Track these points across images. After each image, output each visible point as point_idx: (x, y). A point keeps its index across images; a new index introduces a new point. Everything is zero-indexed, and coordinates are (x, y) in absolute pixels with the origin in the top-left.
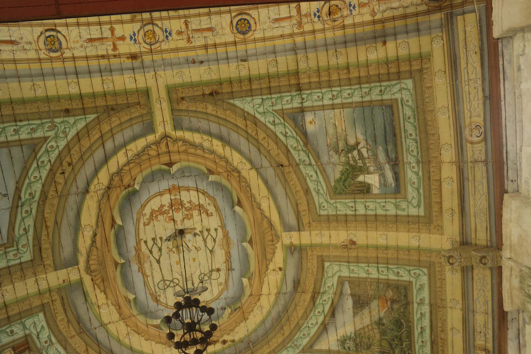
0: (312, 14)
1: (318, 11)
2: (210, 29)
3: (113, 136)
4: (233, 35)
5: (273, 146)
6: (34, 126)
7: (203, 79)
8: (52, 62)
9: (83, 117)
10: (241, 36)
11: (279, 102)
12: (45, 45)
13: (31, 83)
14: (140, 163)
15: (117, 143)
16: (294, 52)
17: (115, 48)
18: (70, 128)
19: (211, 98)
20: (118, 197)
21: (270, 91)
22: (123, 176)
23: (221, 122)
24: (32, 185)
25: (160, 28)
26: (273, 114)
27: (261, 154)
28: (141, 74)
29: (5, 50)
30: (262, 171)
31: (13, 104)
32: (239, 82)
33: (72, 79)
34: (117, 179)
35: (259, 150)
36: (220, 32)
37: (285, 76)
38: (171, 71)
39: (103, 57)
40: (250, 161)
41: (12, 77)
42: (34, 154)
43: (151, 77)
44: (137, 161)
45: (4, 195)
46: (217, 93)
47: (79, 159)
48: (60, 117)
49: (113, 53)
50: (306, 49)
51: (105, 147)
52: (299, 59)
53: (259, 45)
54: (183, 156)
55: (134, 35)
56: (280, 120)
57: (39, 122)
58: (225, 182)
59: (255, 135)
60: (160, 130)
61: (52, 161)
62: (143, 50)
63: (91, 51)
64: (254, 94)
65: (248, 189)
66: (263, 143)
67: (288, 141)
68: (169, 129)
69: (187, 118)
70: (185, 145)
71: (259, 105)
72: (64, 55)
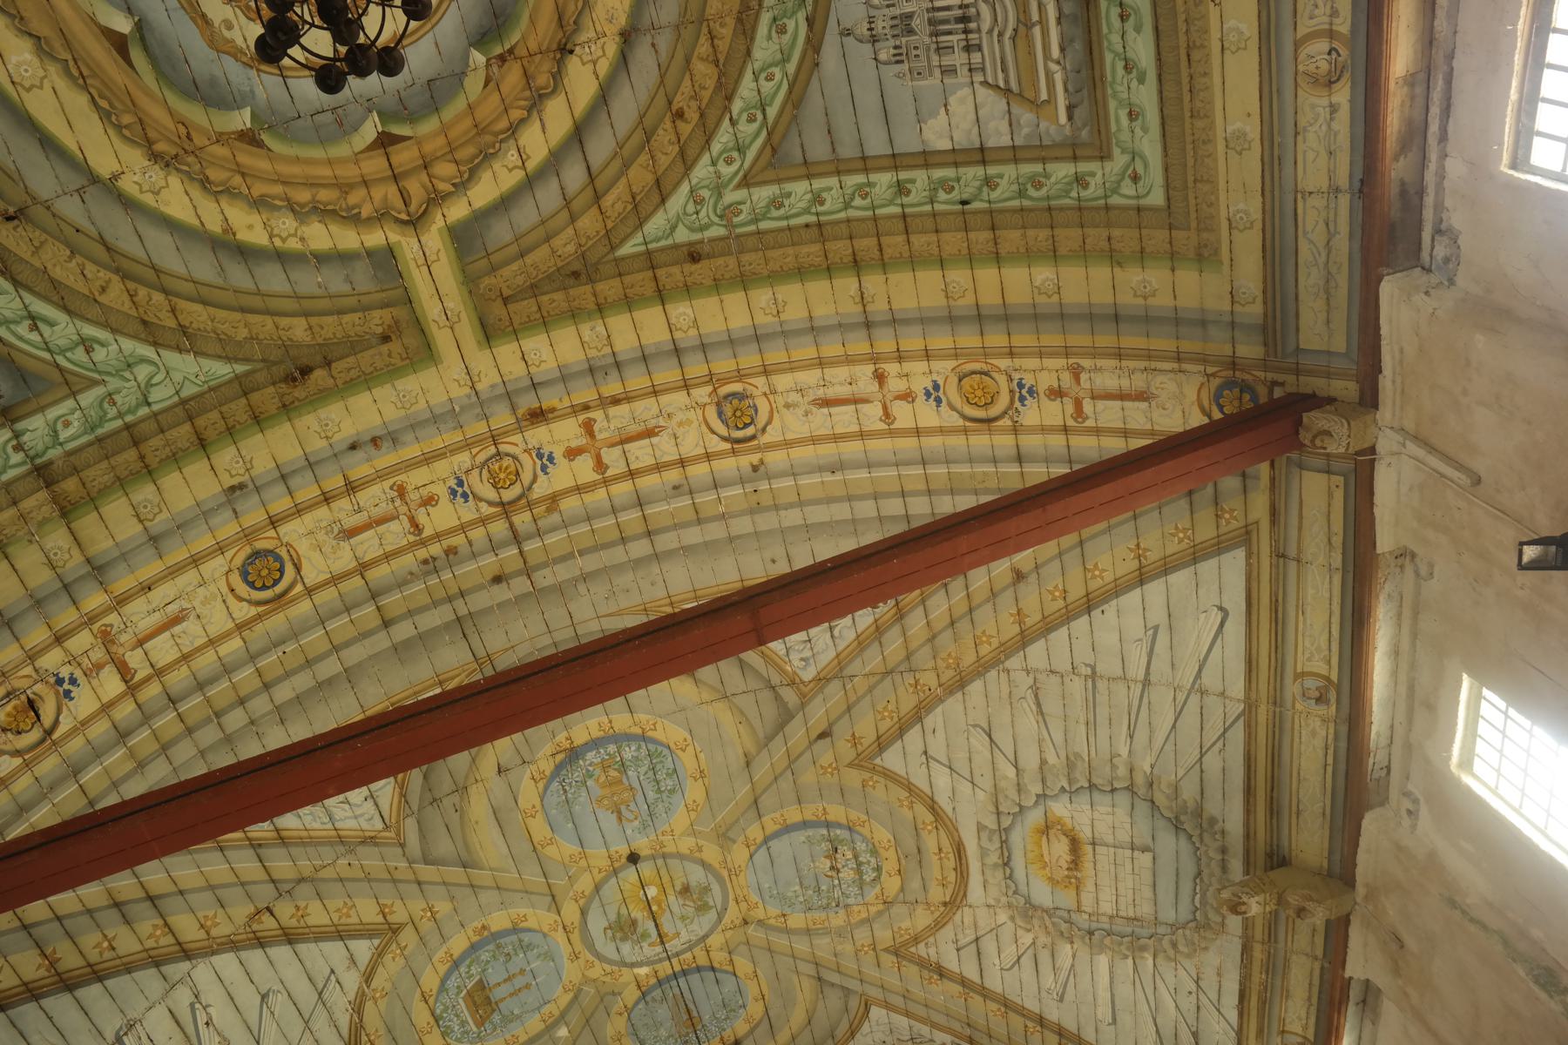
0: (81, 679)
1: (67, 694)
2: (350, 533)
3: (568, 203)
4: (284, 541)
5: (66, 272)
6: (775, 213)
7: (340, 404)
8: (738, 371)
9: (650, 246)
10: (261, 545)
11: (93, 413)
12: (755, 406)
13: (783, 317)
14: (478, 134)
15: (554, 184)
16: (98, 563)
17: (588, 427)
18: (685, 213)
19: (305, 361)
20: (532, 21)
21: (133, 435)
22: (523, 90)
23: (257, 302)
24: (779, 56)
25: (481, 500)
26: (99, 373)
27: (97, 237)
28: (512, 377)
29: (841, 384)
30: (77, 181)
31: (825, 266)
32: (234, 426)
33: (687, 337)
34: (542, 79)
35: (108, 249)
36: (321, 536)
37: (100, 490)
38: (431, 403)
39: (616, 401)
40: (127, 203)
41: (827, 329)
42: (776, 138)
43: (482, 375)
44: (488, 138)
45: (849, 34)
46: (290, 379)
47: (655, 129)
48: (712, 240)
49: (591, 415)
50: (66, 587)
51: (585, 170)
52: (76, 552)
53: (205, 542)
54: (349, 172)
55: (544, 469)
56: (68, 360)
57: (764, 225)
58: (194, 113)
59: (136, 291)
60: (434, 237)
61: (726, 122)
62: (517, 438)
63: (646, 409)
64: (179, 410)
65: (103, 104)
66: (101, 274)
67: (17, 304)
68: (407, 245)
69: (360, 288)
70: (349, 209)
71: (154, 381)
72: (709, 388)
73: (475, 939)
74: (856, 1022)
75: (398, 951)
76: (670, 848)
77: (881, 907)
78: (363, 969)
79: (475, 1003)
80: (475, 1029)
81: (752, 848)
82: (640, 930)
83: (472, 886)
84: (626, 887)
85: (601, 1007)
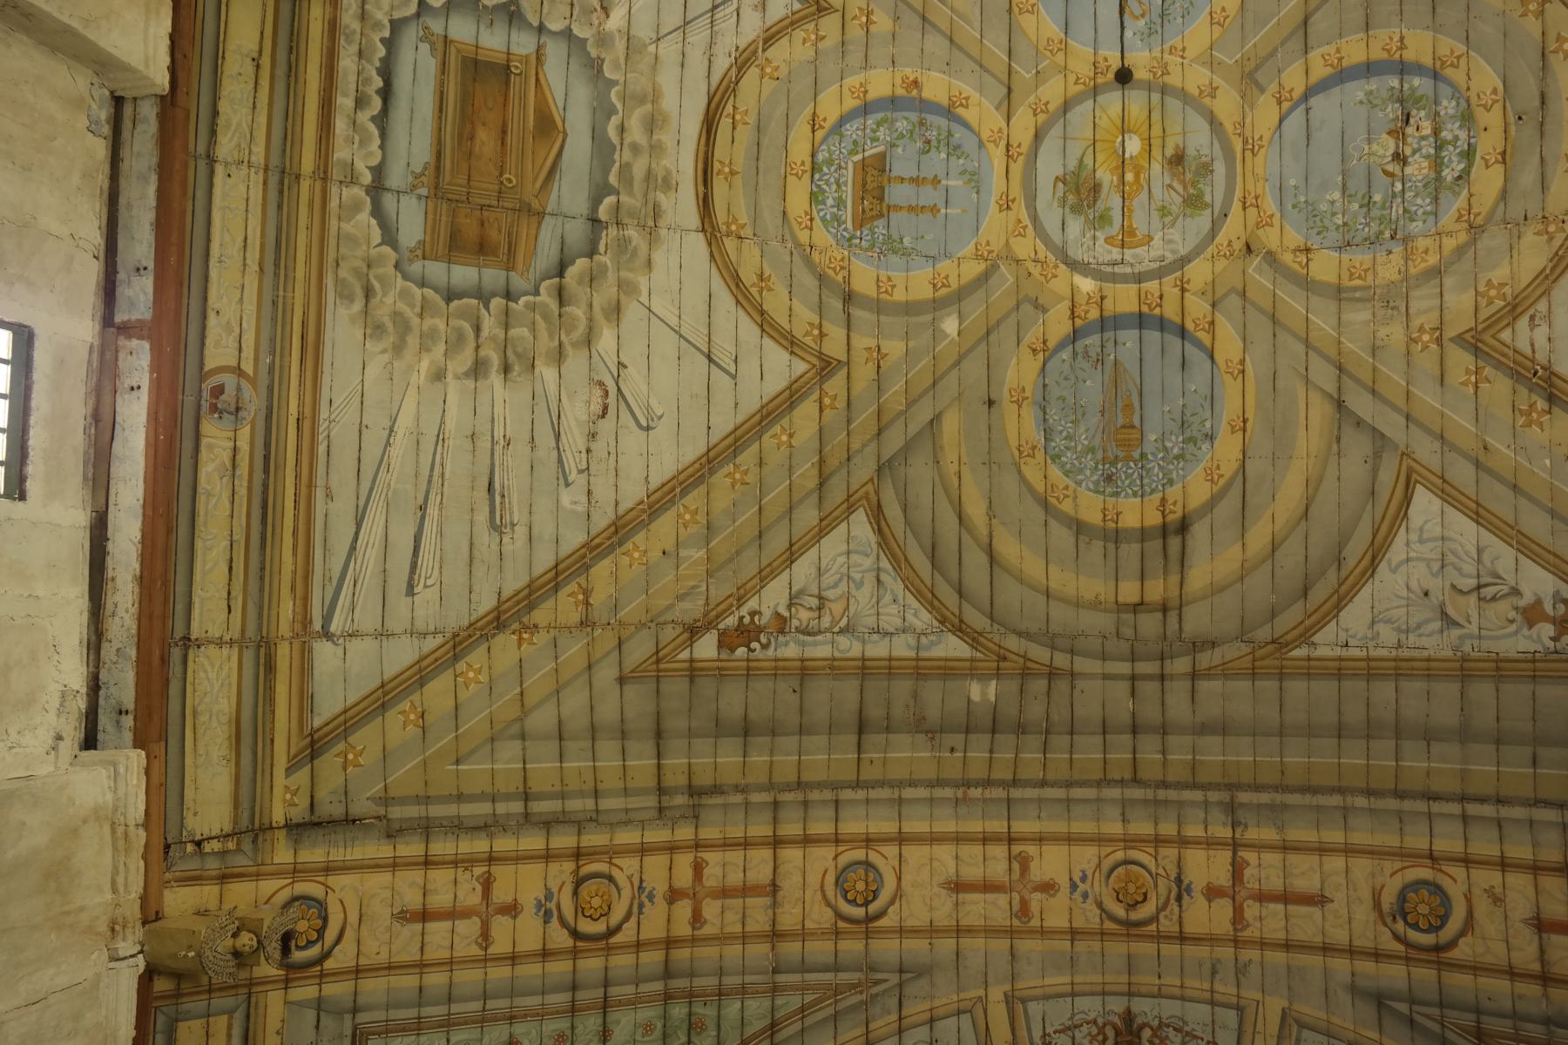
73: (900, 92)
74: (1384, 527)
75: (813, 37)
76: (1174, 80)
77: (1463, 237)
78: (769, 24)
79: (864, 185)
80: (849, 225)
81: (1286, 105)
82: (1100, 205)
83: (924, 18)
84: (1103, 122)
85: (1012, 320)
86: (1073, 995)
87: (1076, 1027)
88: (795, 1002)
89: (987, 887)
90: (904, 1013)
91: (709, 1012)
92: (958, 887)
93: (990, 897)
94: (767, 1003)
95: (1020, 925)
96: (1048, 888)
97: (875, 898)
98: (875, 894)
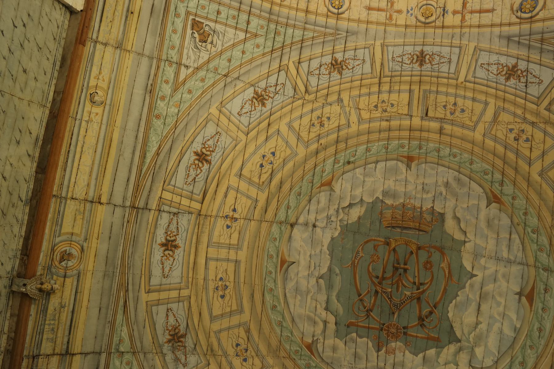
86: (404, 45)
87: (404, 55)
88: (311, 35)
89: (379, 10)
90: (346, 46)
91: (282, 30)
92: (369, 9)
93: (379, 13)
94: (302, 33)
95: (389, 22)
96: (399, 12)
97: (341, 8)
98: (342, 6)
